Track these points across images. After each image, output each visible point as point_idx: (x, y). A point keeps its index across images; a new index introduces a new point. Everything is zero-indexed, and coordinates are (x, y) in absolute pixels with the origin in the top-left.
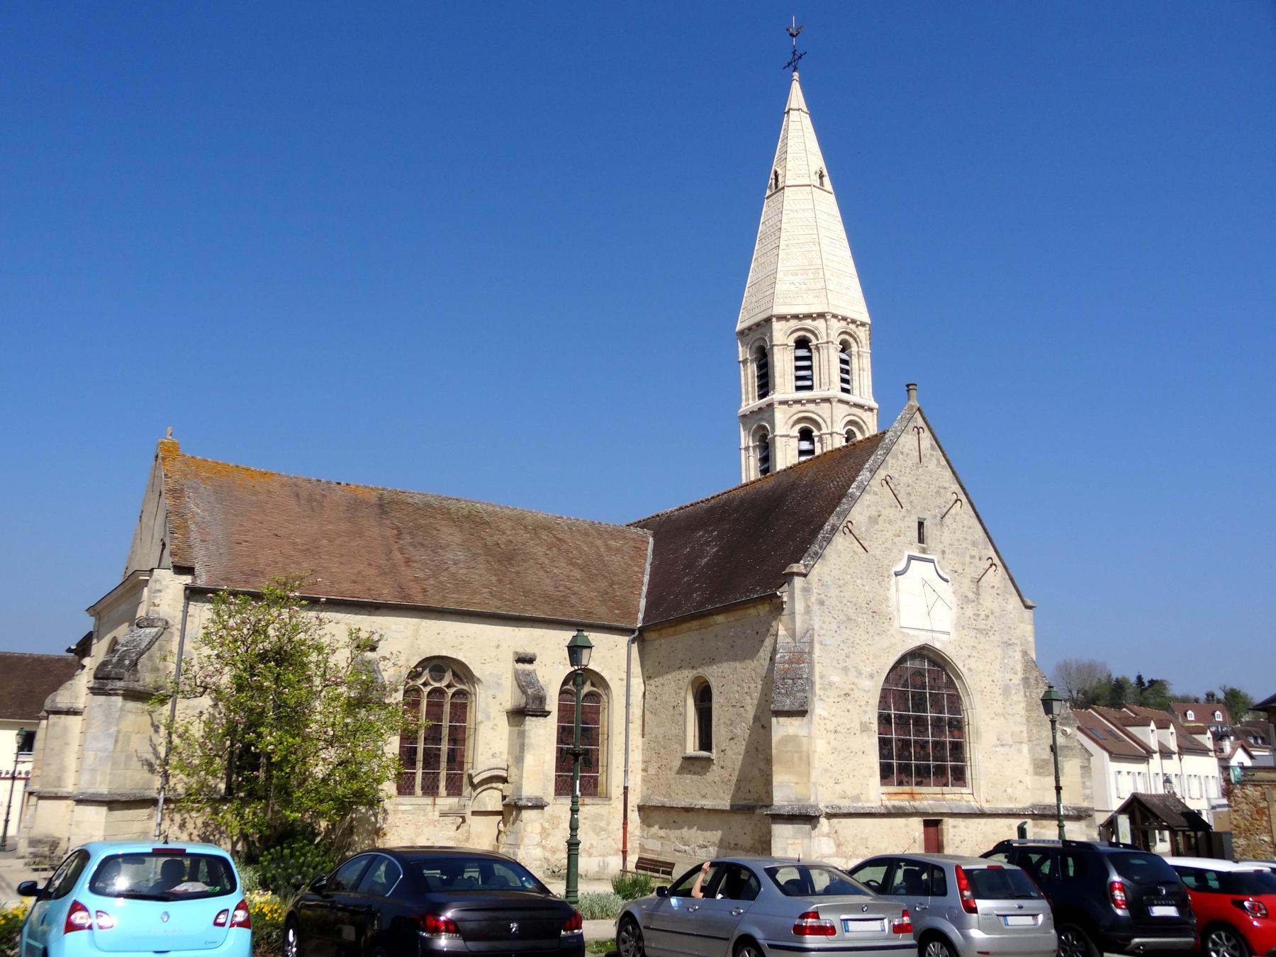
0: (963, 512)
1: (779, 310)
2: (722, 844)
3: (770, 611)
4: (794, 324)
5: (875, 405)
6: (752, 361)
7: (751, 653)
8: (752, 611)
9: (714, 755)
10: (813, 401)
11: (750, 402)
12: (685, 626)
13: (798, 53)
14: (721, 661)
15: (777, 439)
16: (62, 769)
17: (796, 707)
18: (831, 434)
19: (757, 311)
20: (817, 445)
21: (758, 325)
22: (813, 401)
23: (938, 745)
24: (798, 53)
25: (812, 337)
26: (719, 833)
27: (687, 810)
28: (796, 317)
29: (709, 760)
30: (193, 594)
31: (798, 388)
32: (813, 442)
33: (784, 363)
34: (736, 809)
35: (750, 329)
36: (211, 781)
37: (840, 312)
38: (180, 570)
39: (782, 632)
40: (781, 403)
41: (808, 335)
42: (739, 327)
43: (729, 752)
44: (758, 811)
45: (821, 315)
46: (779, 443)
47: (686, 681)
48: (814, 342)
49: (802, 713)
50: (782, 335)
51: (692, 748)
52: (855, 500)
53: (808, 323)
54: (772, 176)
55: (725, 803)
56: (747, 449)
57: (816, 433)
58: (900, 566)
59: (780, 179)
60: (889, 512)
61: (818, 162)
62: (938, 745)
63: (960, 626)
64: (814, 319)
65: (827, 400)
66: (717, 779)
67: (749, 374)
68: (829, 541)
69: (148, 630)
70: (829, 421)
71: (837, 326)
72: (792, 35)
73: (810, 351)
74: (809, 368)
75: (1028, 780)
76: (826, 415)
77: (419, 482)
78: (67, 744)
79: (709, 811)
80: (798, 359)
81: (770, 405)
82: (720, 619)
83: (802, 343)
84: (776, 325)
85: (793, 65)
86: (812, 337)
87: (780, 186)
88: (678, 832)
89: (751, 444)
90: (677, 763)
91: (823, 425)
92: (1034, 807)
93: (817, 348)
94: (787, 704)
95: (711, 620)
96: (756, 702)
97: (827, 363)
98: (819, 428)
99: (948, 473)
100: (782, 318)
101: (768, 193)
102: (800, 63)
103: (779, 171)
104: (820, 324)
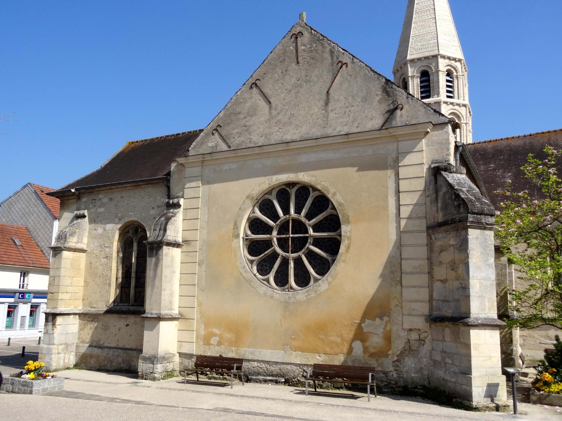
1: (442, 52)
6: (417, 77)
16: (172, 295)
18: (466, 124)
19: (425, 50)
21: (427, 58)
22: (458, 105)
25: (454, 71)
28: (449, 58)
31: (448, 97)
35: (419, 59)
41: (452, 69)
42: (409, 57)
48: (455, 74)
50: (443, 65)
53: (453, 63)
70: (465, 116)
78: (174, 272)
81: (438, 103)
84: (441, 60)
86: (454, 71)
88: (543, 333)
91: (462, 118)
100: (443, 57)
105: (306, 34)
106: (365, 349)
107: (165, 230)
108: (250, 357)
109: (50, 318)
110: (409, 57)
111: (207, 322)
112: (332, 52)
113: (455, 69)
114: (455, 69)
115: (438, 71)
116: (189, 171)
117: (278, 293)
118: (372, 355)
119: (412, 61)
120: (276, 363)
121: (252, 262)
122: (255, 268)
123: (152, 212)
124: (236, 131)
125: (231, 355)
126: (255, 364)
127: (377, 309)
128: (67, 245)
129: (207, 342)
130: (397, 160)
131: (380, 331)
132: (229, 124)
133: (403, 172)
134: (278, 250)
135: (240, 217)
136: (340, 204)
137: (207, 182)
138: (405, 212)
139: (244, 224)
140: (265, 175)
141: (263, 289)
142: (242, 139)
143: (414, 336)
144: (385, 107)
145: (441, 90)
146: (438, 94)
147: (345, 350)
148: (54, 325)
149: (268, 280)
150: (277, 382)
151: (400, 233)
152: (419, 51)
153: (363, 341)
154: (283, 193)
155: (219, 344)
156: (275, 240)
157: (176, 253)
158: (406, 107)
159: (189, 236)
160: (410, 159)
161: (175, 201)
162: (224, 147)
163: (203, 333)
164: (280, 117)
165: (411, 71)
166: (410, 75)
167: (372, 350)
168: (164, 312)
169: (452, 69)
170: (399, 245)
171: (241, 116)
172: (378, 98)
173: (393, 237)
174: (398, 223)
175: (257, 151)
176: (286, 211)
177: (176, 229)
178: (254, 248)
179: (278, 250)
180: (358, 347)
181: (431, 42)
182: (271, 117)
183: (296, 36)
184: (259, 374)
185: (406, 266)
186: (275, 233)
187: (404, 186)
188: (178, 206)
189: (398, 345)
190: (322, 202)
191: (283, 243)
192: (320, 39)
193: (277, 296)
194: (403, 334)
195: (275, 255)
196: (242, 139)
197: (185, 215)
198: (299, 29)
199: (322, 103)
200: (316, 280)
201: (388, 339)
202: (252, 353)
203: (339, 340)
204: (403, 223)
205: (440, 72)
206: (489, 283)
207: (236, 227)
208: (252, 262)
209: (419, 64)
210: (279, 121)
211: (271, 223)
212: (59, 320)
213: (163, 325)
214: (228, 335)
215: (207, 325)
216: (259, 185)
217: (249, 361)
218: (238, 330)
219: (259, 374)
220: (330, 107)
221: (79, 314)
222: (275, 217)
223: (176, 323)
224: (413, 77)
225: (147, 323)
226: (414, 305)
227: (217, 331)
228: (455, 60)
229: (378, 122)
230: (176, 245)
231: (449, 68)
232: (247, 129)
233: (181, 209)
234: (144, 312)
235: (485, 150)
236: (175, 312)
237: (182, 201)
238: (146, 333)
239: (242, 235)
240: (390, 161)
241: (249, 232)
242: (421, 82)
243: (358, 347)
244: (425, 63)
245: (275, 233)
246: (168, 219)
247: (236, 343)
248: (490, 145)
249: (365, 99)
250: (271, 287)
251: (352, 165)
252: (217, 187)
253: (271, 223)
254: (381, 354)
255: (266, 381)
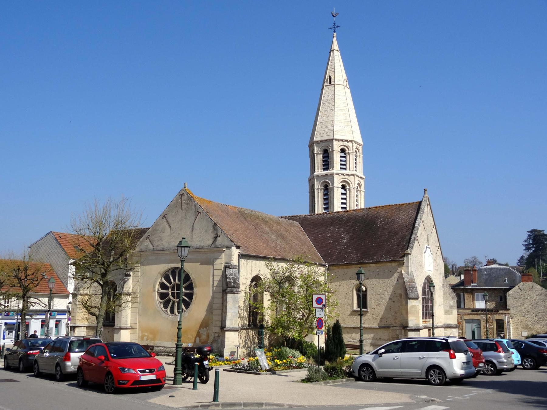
0: (434, 231)
1: (336, 137)
2: (373, 339)
3: (398, 265)
4: (341, 143)
5: (364, 177)
6: (320, 154)
7: (389, 277)
8: (389, 264)
9: (369, 310)
10: (348, 175)
11: (319, 171)
12: (353, 266)
13: (336, 25)
14: (372, 279)
15: (335, 188)
17: (416, 297)
18: (354, 188)
19: (326, 134)
20: (348, 192)
21: (326, 140)
22: (348, 175)
23: (428, 306)
24: (336, 25)
25: (347, 149)
26: (372, 335)
27: (354, 328)
28: (342, 140)
29: (367, 311)
30: (242, 256)
31: (341, 168)
32: (345, 190)
33: (337, 157)
34: (380, 327)
35: (321, 141)
36: (246, 322)
37: (357, 140)
38: (238, 247)
39: (403, 272)
40: (337, 174)
41: (345, 148)
43: (376, 310)
44: (392, 328)
45: (351, 141)
46: (335, 189)
47: (353, 285)
48: (347, 151)
49: (417, 298)
50: (337, 146)
51: (355, 307)
52: (418, 229)
53: (346, 143)
54: (327, 77)
55: (376, 326)
56: (318, 189)
57: (348, 187)
58: (424, 251)
59: (332, 80)
60: (424, 233)
61: (345, 77)
62: (428, 306)
63: (434, 269)
64: (348, 142)
65: (353, 175)
66: (370, 318)
67: (319, 160)
68: (414, 242)
69: (234, 270)
70: (353, 183)
71: (355, 145)
72: (333, 16)
73: (345, 154)
74: (345, 161)
75: (443, 316)
76: (352, 181)
77: (248, 206)
79: (366, 328)
80: (341, 157)
81: (332, 175)
82: (372, 265)
83: (343, 151)
84: (335, 143)
85: (334, 28)
86: (347, 149)
87: (332, 83)
88: (350, 335)
89: (320, 187)
90: (348, 313)
92: (444, 324)
93: (349, 153)
94: (413, 296)
95: (368, 265)
96: (390, 294)
97: (351, 159)
98: (349, 185)
99: (432, 219)
101: (325, 84)
102: (337, 29)
103: (332, 77)
104: (350, 144)
105: (186, 195)
106: (200, 340)
107: (123, 288)
108: (159, 345)
109: (72, 329)
110: (315, 139)
111: (142, 330)
112: (195, 206)
113: (347, 147)
114: (347, 147)
115: (333, 151)
116: (135, 259)
117: (170, 317)
118: (202, 343)
119: (317, 142)
120: (169, 347)
121: (161, 303)
122: (162, 305)
123: (120, 277)
124: (157, 239)
125: (151, 345)
126: (161, 348)
127: (205, 324)
128: (79, 293)
129: (142, 339)
130: (214, 262)
131: (205, 333)
132: (153, 235)
133: (215, 266)
134: (171, 298)
135: (156, 282)
136: (194, 279)
137: (143, 264)
138: (216, 283)
139: (157, 285)
140: (166, 263)
141: (164, 315)
142: (159, 243)
143: (217, 335)
144: (213, 235)
145: (335, 165)
146: (333, 168)
147: (193, 341)
148: (74, 332)
149: (167, 311)
150: (169, 355)
151: (214, 293)
152: (322, 135)
153: (200, 337)
154: (174, 271)
155: (147, 340)
156: (170, 293)
157: (130, 298)
158: (221, 236)
159: (134, 290)
160: (218, 261)
161: (128, 273)
162: (151, 247)
163: (140, 335)
164: (174, 234)
165: (316, 150)
166: (315, 152)
167: (202, 341)
168: (123, 326)
169: (345, 148)
170: (213, 298)
171: (159, 232)
172: (211, 231)
173: (211, 294)
174: (213, 288)
175: (162, 252)
176: (175, 281)
177: (129, 286)
178: (162, 296)
179: (171, 298)
180: (198, 339)
181: (330, 128)
182: (171, 234)
183: (182, 195)
184: (162, 352)
185: (215, 306)
186: (170, 290)
187: (216, 272)
188: (129, 275)
189: (211, 339)
190: (187, 278)
191: (173, 294)
192: (191, 199)
193: (169, 318)
194: (213, 334)
195: (170, 300)
196: (159, 243)
197: (133, 280)
198: (183, 192)
199: (191, 230)
200: (185, 311)
201: (208, 336)
202: (160, 343)
203: (191, 337)
204: (214, 288)
205: (334, 152)
206: (235, 314)
207: (154, 287)
208: (161, 303)
209: (322, 144)
210: (174, 236)
211: (168, 285)
212: (77, 329)
213: (122, 331)
214: (151, 336)
215: (142, 332)
216: (164, 267)
217: (156, 346)
218: (154, 333)
219: (162, 352)
220: (194, 233)
221: (86, 327)
222: (170, 282)
223: (129, 330)
224: (317, 154)
225: (115, 330)
226: (217, 323)
227: (146, 334)
228: (347, 141)
229: (210, 242)
230: (129, 294)
231: (343, 147)
232: (161, 239)
233: (131, 277)
234: (114, 326)
235: (342, 217)
236: (129, 325)
237: (131, 273)
238: (115, 335)
239: (157, 290)
240: (212, 261)
241: (160, 289)
242: (324, 157)
243: (198, 339)
244: (325, 144)
245: (170, 290)
246: (125, 282)
247: (154, 339)
248: (346, 214)
249: (206, 231)
250: (168, 314)
251: (198, 262)
252: (147, 267)
253: (168, 285)
254: (205, 342)
255: (164, 355)
